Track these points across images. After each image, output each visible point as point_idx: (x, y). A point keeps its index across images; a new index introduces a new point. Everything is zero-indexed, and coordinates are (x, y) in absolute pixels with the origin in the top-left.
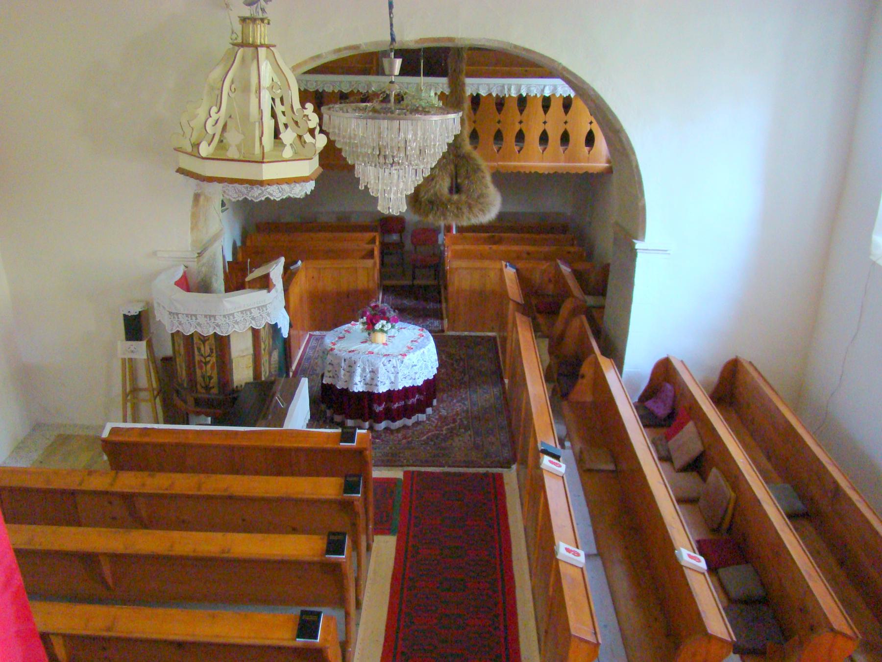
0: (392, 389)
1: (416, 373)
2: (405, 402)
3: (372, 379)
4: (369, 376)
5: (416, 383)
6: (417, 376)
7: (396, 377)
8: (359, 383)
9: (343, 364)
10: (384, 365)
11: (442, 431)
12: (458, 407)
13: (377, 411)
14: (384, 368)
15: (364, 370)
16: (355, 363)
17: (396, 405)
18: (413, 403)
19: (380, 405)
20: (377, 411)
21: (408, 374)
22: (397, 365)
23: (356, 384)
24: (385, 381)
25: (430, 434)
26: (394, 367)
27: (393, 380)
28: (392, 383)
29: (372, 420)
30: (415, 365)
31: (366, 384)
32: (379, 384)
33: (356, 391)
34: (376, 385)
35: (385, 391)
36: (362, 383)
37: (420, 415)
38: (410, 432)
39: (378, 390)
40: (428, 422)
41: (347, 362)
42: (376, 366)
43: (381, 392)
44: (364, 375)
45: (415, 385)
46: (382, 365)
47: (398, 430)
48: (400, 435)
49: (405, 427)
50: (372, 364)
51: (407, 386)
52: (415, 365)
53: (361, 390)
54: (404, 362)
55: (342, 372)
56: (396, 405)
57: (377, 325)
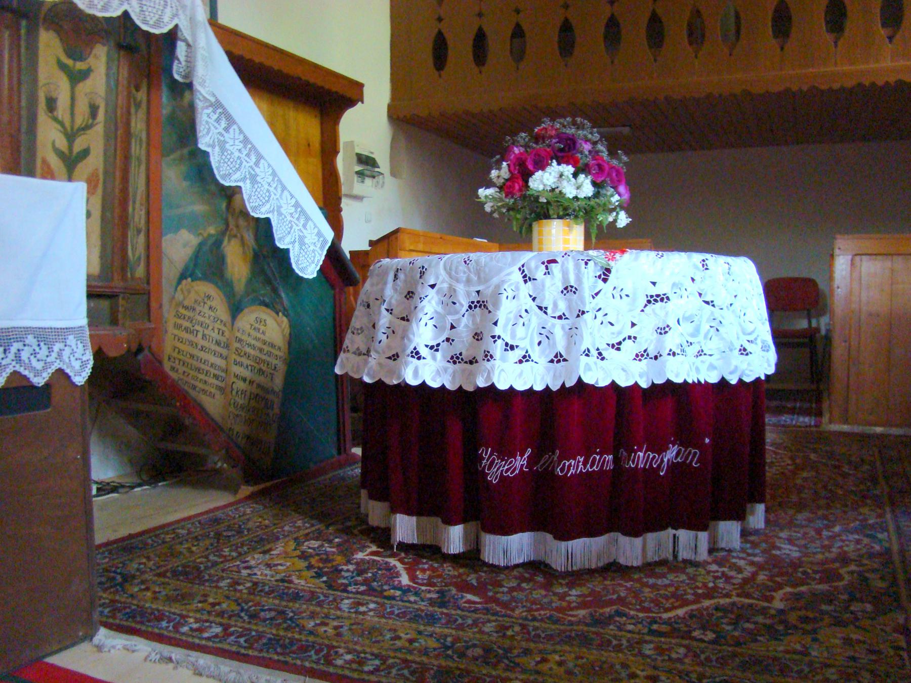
0: (555, 387)
1: (663, 331)
2: (616, 460)
3: (478, 336)
4: (465, 325)
5: (662, 371)
6: (671, 341)
7: (573, 333)
8: (424, 352)
9: (389, 292)
10: (526, 279)
11: (770, 599)
12: (850, 543)
13: (493, 477)
14: (526, 290)
15: (450, 300)
16: (422, 274)
17: (575, 466)
18: (649, 473)
19: (506, 453)
20: (493, 477)
21: (632, 332)
22: (579, 279)
23: (417, 355)
24: (522, 344)
25: (707, 603)
26: (568, 289)
27: (561, 348)
28: (558, 358)
29: (473, 525)
30: (662, 298)
31: (455, 359)
32: (498, 349)
33: (413, 382)
34: (488, 356)
35: (520, 387)
36: (439, 355)
37: (684, 535)
38: (622, 588)
39: (489, 377)
40: (714, 567)
41: (401, 276)
42: (495, 281)
43: (502, 386)
44: (450, 319)
45: (659, 381)
46: (518, 277)
47: (576, 577)
48: (575, 593)
49: (613, 569)
50: (478, 273)
51: (624, 382)
52: (662, 298)
53: (434, 384)
54: (612, 277)
55: (385, 320)
56: (575, 466)
57: (539, 174)
